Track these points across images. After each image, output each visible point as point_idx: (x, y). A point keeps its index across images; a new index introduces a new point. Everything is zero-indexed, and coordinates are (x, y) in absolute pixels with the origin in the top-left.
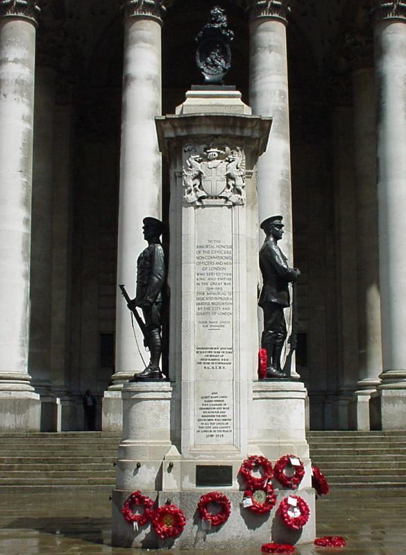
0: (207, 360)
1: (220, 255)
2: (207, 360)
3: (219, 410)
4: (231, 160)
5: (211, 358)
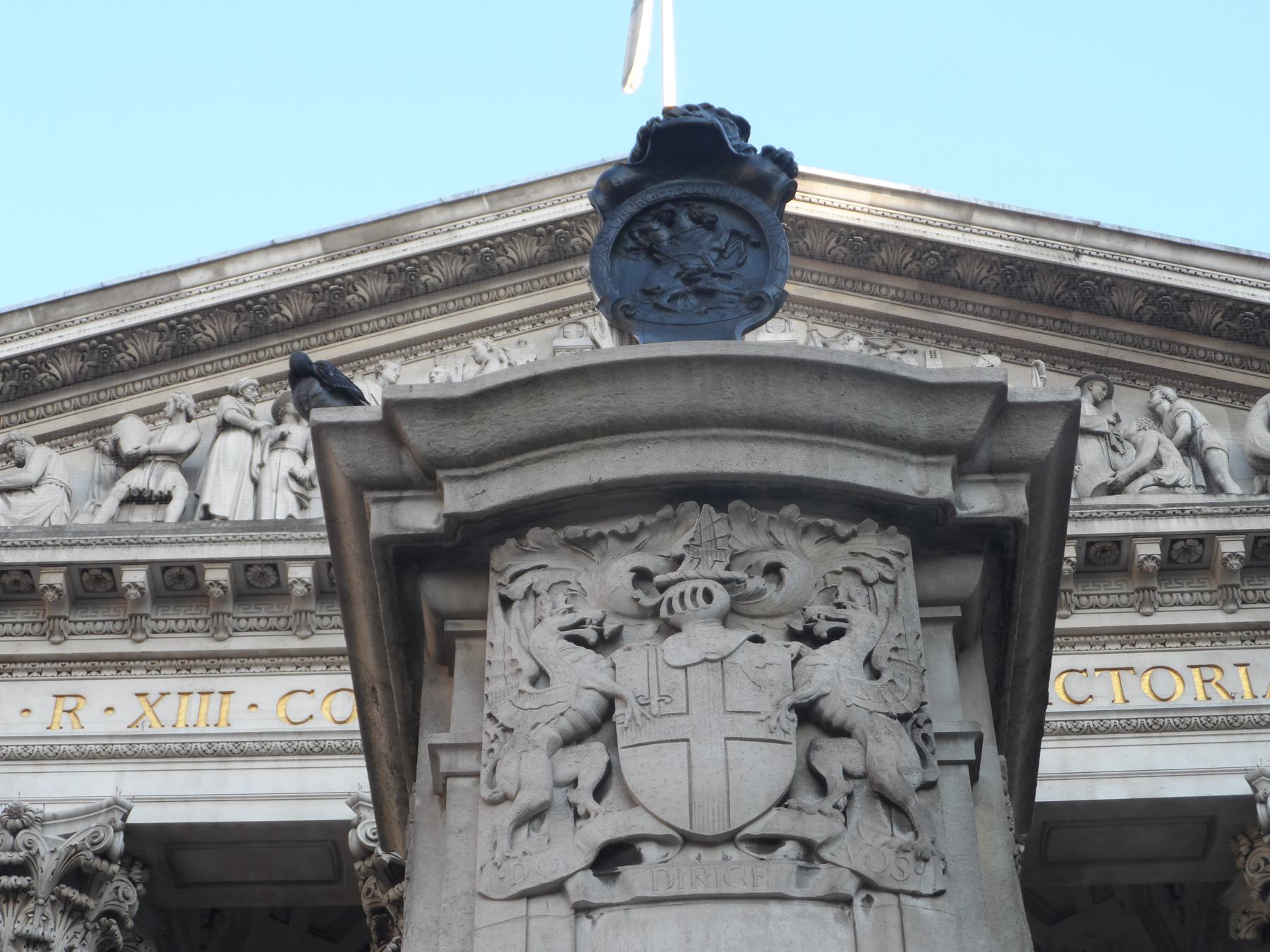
4: (822, 628)
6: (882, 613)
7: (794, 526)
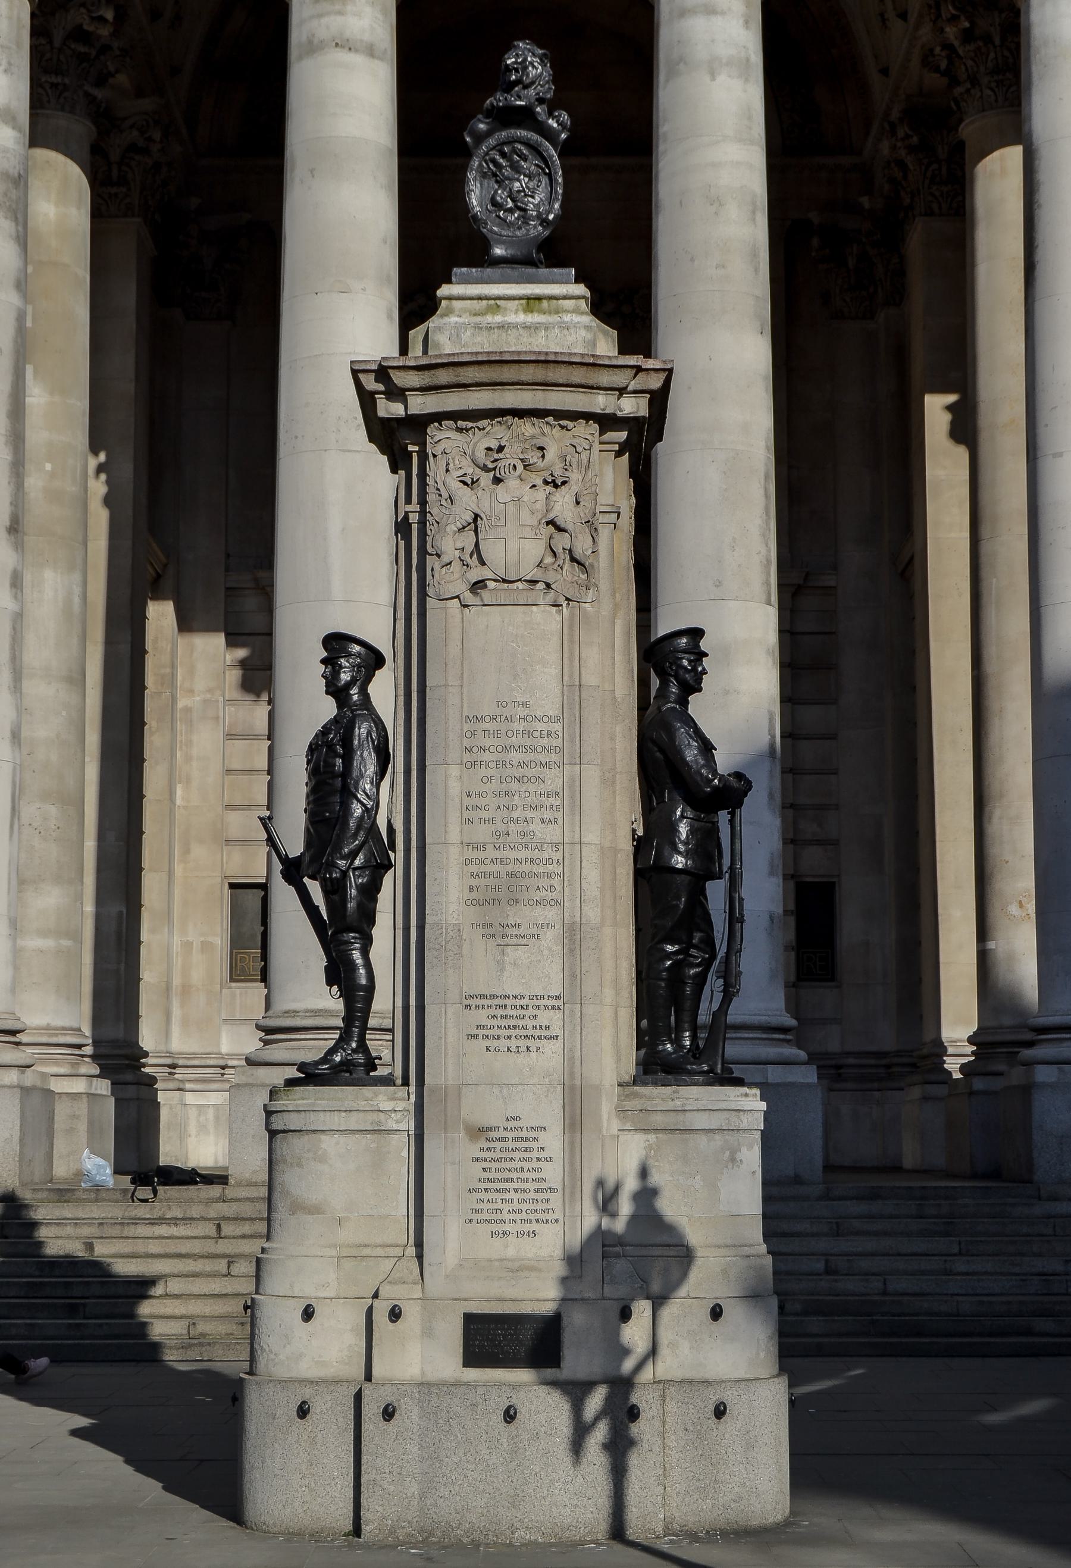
0: (492, 1027)
1: (528, 742)
2: (492, 1027)
3: (525, 1165)
5: (504, 1023)
6: (583, 469)
7: (551, 425)
